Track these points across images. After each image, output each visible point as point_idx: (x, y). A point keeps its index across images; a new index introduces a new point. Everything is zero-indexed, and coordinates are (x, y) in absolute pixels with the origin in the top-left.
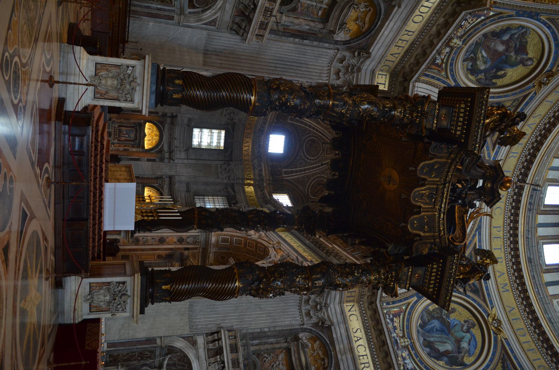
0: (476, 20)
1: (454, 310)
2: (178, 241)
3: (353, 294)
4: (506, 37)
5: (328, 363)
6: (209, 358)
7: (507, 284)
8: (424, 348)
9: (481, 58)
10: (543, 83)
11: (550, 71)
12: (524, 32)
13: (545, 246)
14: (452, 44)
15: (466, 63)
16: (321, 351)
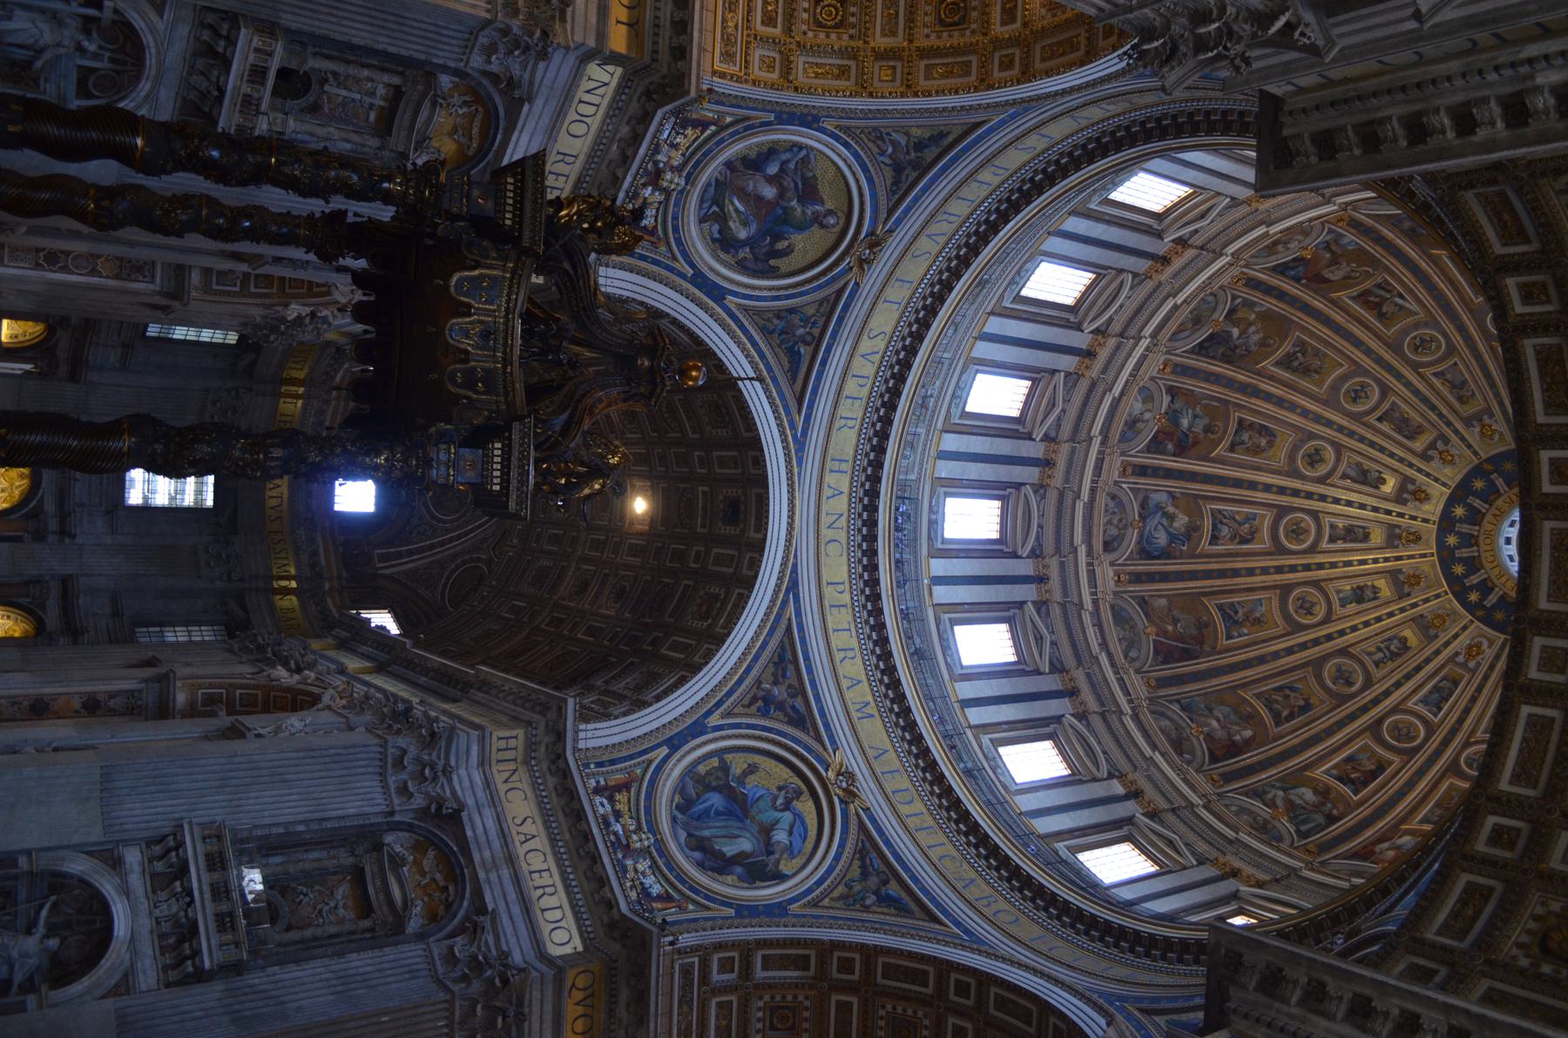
0: (702, 132)
1: (752, 769)
2: (84, 706)
3: (512, 743)
4: (773, 169)
5: (457, 891)
6: (154, 892)
7: (868, 704)
8: (690, 853)
9: (734, 215)
10: (865, 260)
11: (871, 233)
12: (805, 157)
13: (956, 628)
14: (665, 184)
15: (706, 226)
16: (440, 872)
